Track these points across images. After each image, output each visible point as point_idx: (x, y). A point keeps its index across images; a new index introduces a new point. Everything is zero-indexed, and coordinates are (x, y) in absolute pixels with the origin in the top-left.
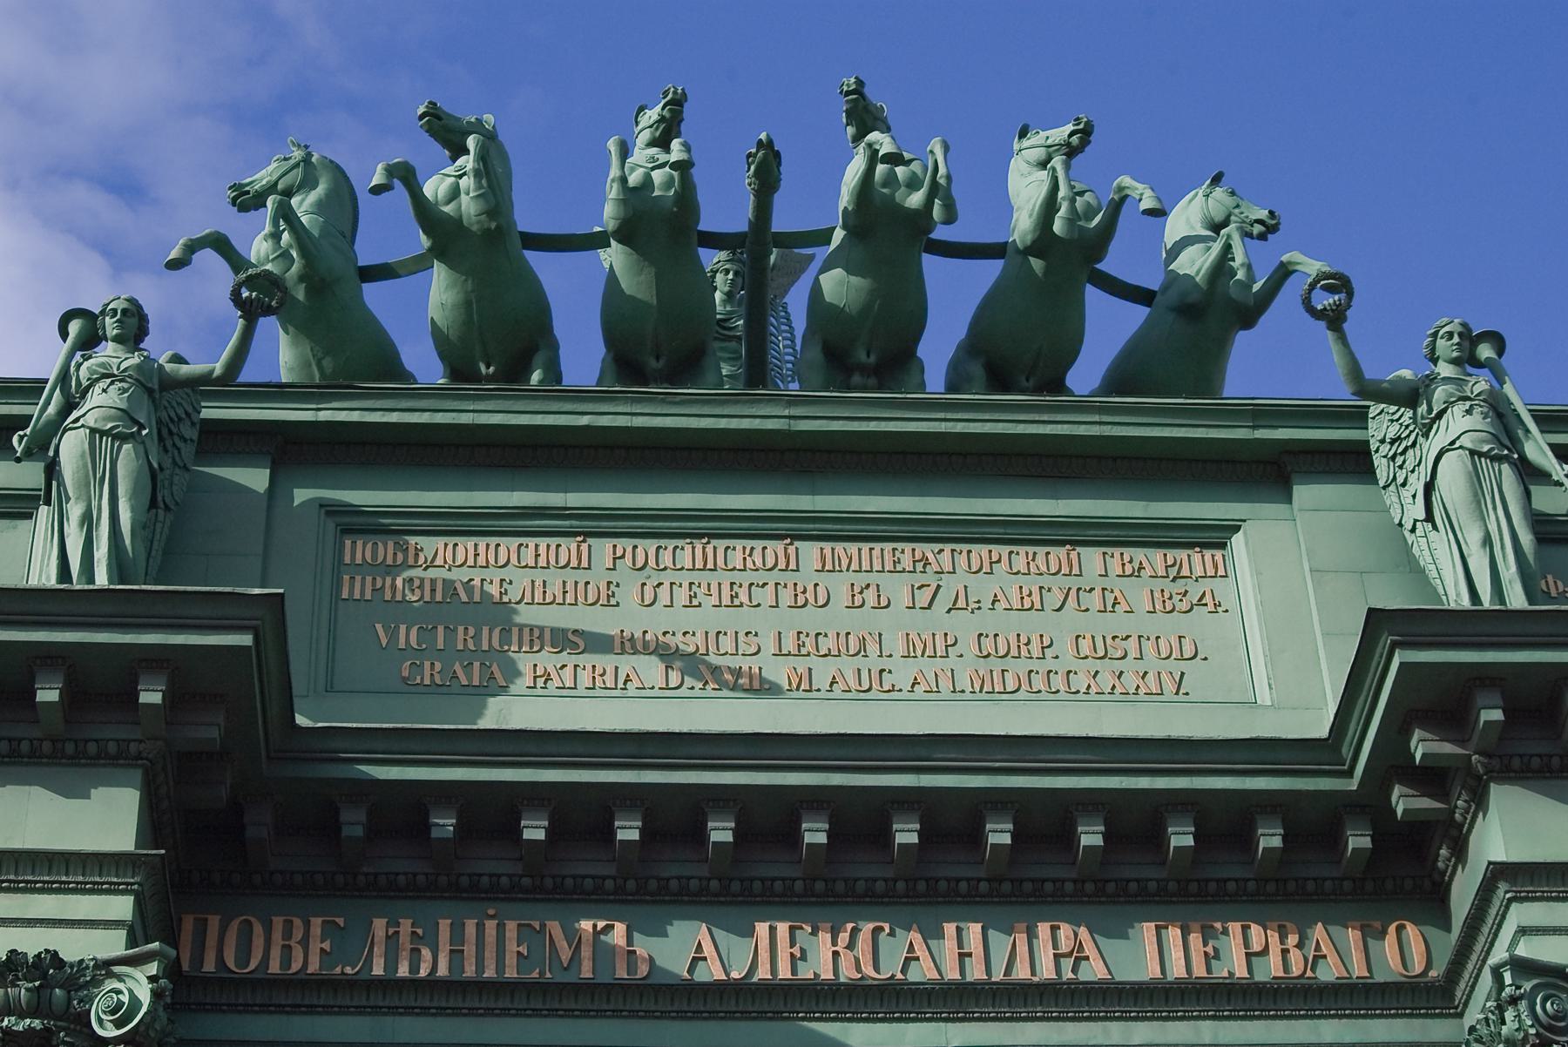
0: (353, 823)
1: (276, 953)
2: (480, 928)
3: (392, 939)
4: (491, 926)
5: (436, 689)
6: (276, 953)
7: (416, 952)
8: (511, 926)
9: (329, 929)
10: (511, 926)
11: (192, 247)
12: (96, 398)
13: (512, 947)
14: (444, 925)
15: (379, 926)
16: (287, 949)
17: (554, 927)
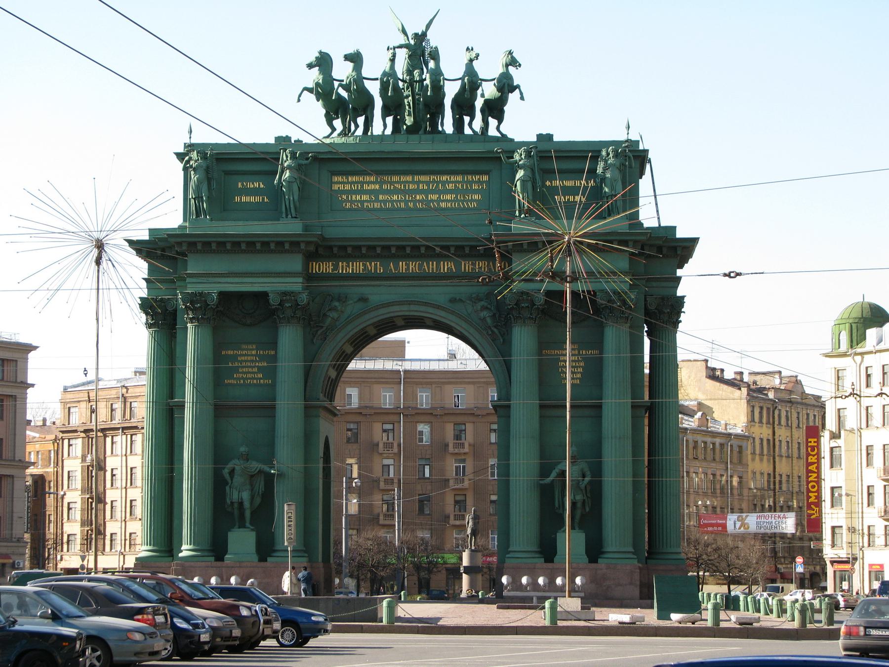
0: (335, 250)
1: (324, 269)
2: (356, 264)
3: (343, 266)
4: (358, 263)
5: (349, 210)
6: (324, 269)
7: (346, 269)
8: (361, 263)
9: (333, 265)
10: (361, 263)
11: (300, 96)
12: (287, 174)
13: (361, 267)
14: (351, 263)
15: (340, 263)
16: (326, 268)
17: (368, 263)
